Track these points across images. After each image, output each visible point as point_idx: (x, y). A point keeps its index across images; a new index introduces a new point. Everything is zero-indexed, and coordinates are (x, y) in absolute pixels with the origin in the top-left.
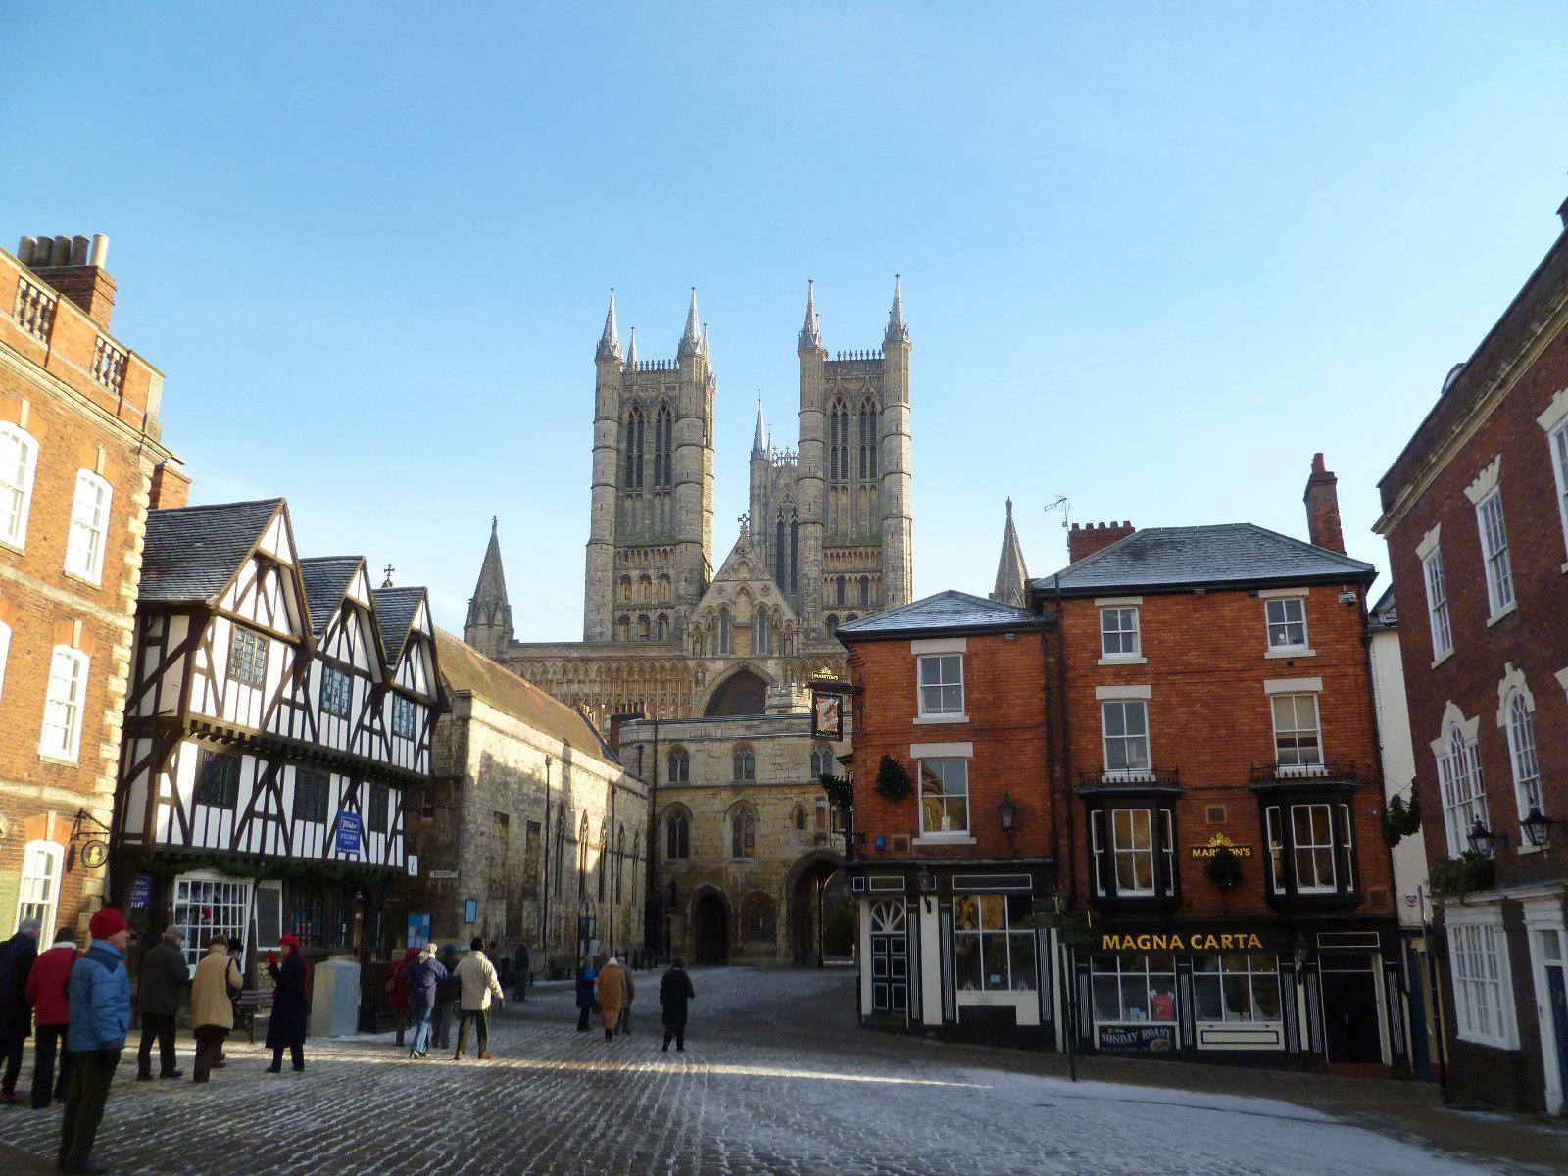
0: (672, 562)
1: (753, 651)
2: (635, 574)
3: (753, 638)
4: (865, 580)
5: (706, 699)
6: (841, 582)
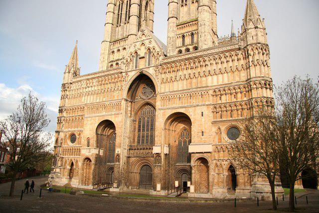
0: (127, 43)
1: (146, 66)
2: (115, 50)
3: (146, 62)
4: (192, 34)
5: (128, 87)
6: (183, 36)
